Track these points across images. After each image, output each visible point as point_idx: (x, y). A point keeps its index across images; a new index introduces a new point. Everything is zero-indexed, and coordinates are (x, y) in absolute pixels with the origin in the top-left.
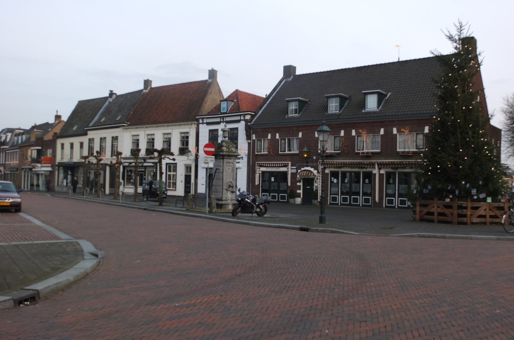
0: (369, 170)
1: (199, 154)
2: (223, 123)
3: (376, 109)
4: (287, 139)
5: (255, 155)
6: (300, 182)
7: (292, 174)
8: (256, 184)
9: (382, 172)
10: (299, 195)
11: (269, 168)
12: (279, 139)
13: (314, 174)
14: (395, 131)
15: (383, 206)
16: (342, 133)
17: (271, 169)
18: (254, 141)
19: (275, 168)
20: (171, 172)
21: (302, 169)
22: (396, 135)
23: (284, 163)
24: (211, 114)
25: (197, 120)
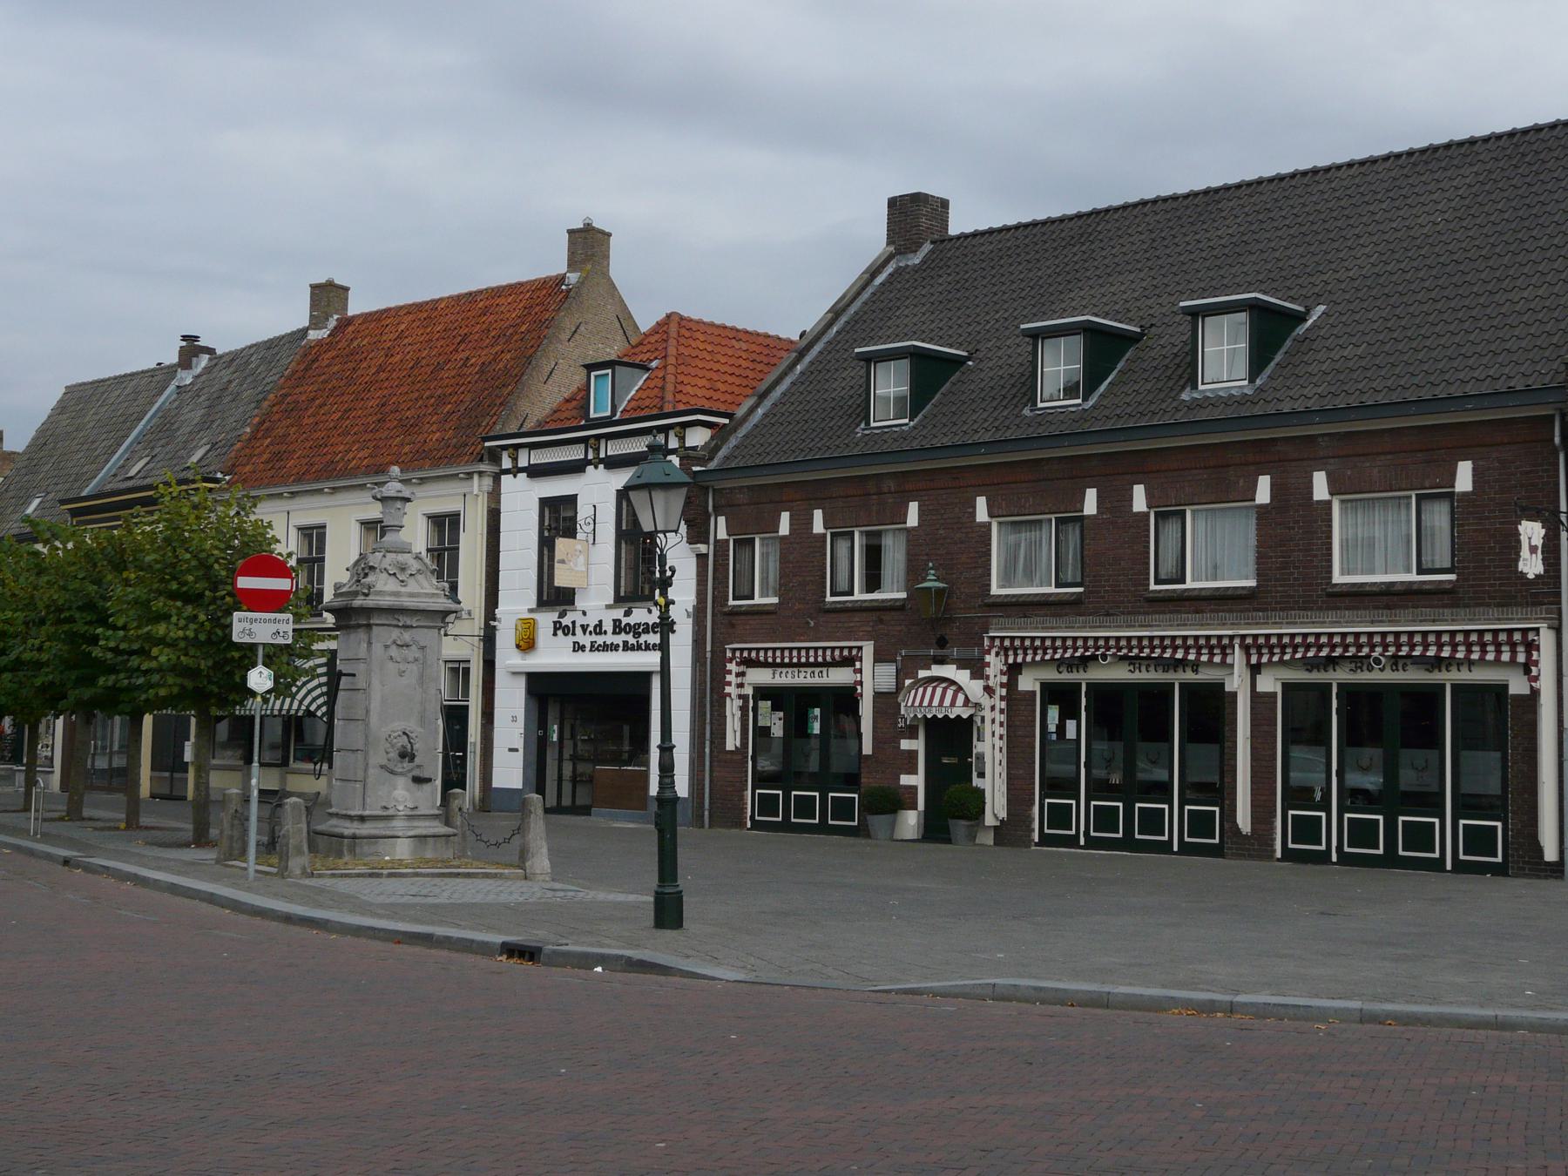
0: (1206, 675)
2: (596, 467)
3: (1245, 383)
4: (861, 532)
5: (726, 609)
6: (911, 733)
7: (878, 696)
8: (730, 746)
9: (1269, 683)
10: (904, 799)
11: (784, 670)
12: (824, 535)
13: (967, 701)
14: (1320, 487)
15: (1274, 851)
16: (1090, 505)
17: (789, 675)
18: (721, 546)
19: (809, 670)
21: (922, 674)
22: (1328, 504)
23: (842, 649)
24: (553, 426)
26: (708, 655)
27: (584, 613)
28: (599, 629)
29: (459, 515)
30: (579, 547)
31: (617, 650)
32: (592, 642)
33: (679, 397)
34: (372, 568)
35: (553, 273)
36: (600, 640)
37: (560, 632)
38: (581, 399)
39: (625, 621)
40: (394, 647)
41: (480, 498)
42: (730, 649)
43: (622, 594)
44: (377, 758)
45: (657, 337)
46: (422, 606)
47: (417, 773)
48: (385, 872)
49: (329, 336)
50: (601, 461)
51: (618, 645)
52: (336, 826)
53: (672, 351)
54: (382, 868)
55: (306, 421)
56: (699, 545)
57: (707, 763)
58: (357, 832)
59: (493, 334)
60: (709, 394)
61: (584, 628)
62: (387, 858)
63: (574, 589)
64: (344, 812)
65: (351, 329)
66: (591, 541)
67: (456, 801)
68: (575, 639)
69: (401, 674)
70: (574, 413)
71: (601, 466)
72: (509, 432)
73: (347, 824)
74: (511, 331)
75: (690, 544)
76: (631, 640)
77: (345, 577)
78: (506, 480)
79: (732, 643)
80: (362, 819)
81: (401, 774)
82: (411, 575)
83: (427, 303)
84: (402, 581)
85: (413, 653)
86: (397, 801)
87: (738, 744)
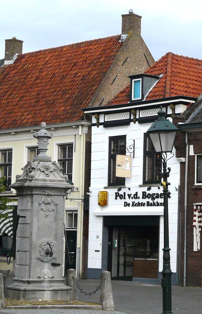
2: (135, 123)
18: (191, 159)
25: (88, 118)
26: (186, 208)
27: (129, 189)
28: (136, 196)
29: (73, 144)
30: (127, 159)
31: (144, 206)
32: (133, 202)
33: (172, 91)
34: (33, 169)
35: (115, 34)
36: (136, 201)
37: (118, 198)
38: (128, 92)
39: (148, 192)
40: (43, 204)
41: (82, 137)
42: (195, 205)
43: (147, 180)
44: (36, 255)
45: (162, 63)
46: (56, 186)
47: (53, 261)
48: (39, 306)
49: (14, 63)
50: (137, 120)
51: (144, 204)
52: (17, 286)
53: (169, 70)
54: (38, 305)
55: (3, 102)
56: (181, 158)
57: (185, 257)
58: (27, 288)
59: (88, 62)
60: (186, 89)
61: (129, 196)
62: (40, 300)
63: (125, 178)
64: (21, 279)
65: (24, 60)
66: (133, 156)
67: (71, 274)
68: (125, 201)
69: (46, 216)
70: (125, 98)
71: (137, 122)
72: (95, 107)
73: (22, 284)
74: (96, 61)
75: (177, 157)
76: (150, 201)
77: (21, 173)
78: (94, 128)
79: (196, 203)
80: (29, 282)
81: (46, 262)
82: (51, 172)
83: (58, 48)
84: (47, 174)
85: (52, 207)
86: (44, 274)
87: (199, 248)
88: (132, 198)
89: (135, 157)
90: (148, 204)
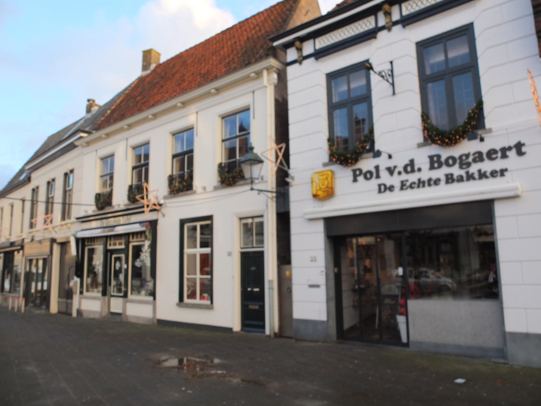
1: (291, 172)
20: (195, 247)
27: (390, 157)
36: (413, 178)
37: (361, 179)
61: (391, 171)
68: (380, 181)
88: (400, 173)
89: (396, 91)
90: (450, 179)
